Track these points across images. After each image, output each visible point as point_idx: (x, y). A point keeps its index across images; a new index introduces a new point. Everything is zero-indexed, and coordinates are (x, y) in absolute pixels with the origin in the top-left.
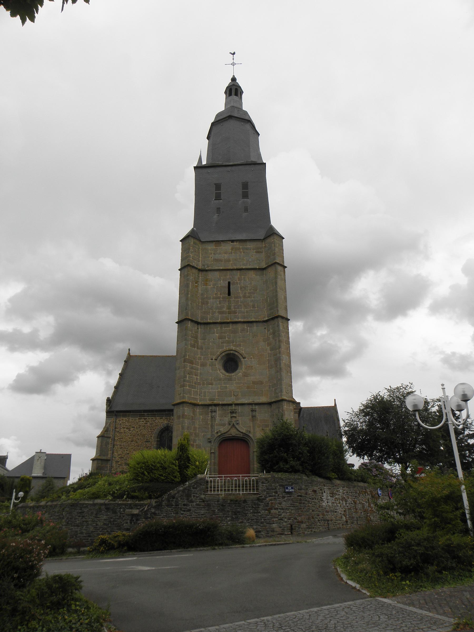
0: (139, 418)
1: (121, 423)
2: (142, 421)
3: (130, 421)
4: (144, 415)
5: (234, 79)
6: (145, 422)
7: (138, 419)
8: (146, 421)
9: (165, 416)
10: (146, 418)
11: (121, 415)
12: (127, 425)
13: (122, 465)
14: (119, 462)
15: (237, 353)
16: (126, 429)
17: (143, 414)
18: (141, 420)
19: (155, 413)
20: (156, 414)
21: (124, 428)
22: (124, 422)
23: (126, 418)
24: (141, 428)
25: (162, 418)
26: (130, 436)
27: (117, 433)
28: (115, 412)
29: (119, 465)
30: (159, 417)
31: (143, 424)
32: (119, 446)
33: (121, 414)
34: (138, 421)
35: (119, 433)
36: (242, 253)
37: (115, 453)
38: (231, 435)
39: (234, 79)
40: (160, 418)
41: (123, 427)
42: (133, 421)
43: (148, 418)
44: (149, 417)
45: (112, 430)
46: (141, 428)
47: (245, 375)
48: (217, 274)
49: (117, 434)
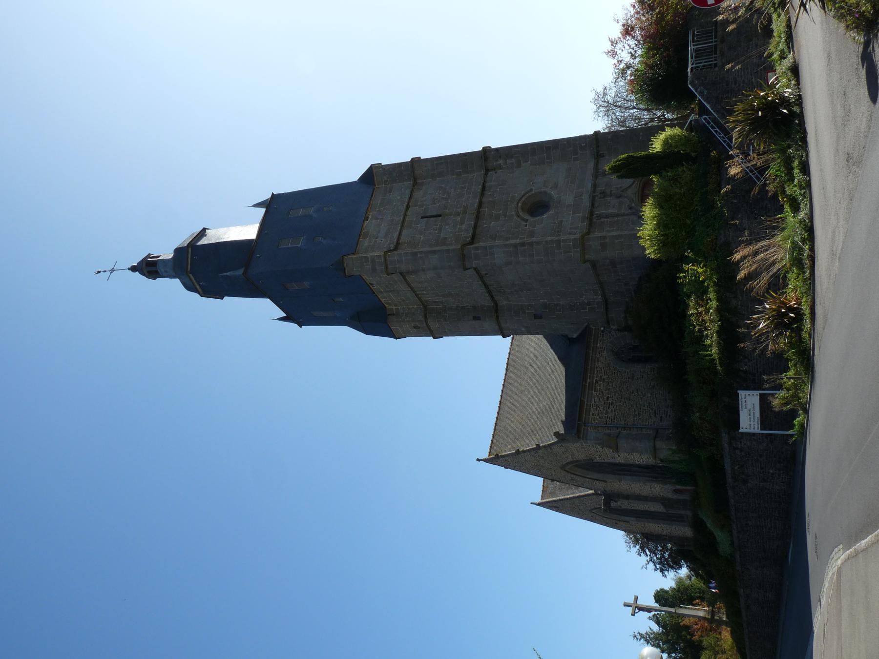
4: (589, 383)
5: (133, 269)
7: (595, 391)
8: (600, 381)
9: (596, 354)
10: (594, 381)
12: (602, 407)
13: (667, 412)
14: (662, 417)
15: (523, 199)
16: (609, 409)
17: (588, 385)
18: (597, 389)
19: (589, 367)
20: (591, 367)
22: (597, 412)
23: (592, 409)
24: (611, 388)
25: (598, 359)
29: (666, 417)
30: (597, 363)
31: (604, 385)
32: (636, 418)
34: (598, 393)
35: (614, 419)
36: (387, 207)
37: (647, 423)
38: (636, 193)
39: (133, 269)
40: (598, 361)
42: (598, 400)
44: (593, 377)
46: (611, 388)
47: (556, 186)
48: (404, 232)
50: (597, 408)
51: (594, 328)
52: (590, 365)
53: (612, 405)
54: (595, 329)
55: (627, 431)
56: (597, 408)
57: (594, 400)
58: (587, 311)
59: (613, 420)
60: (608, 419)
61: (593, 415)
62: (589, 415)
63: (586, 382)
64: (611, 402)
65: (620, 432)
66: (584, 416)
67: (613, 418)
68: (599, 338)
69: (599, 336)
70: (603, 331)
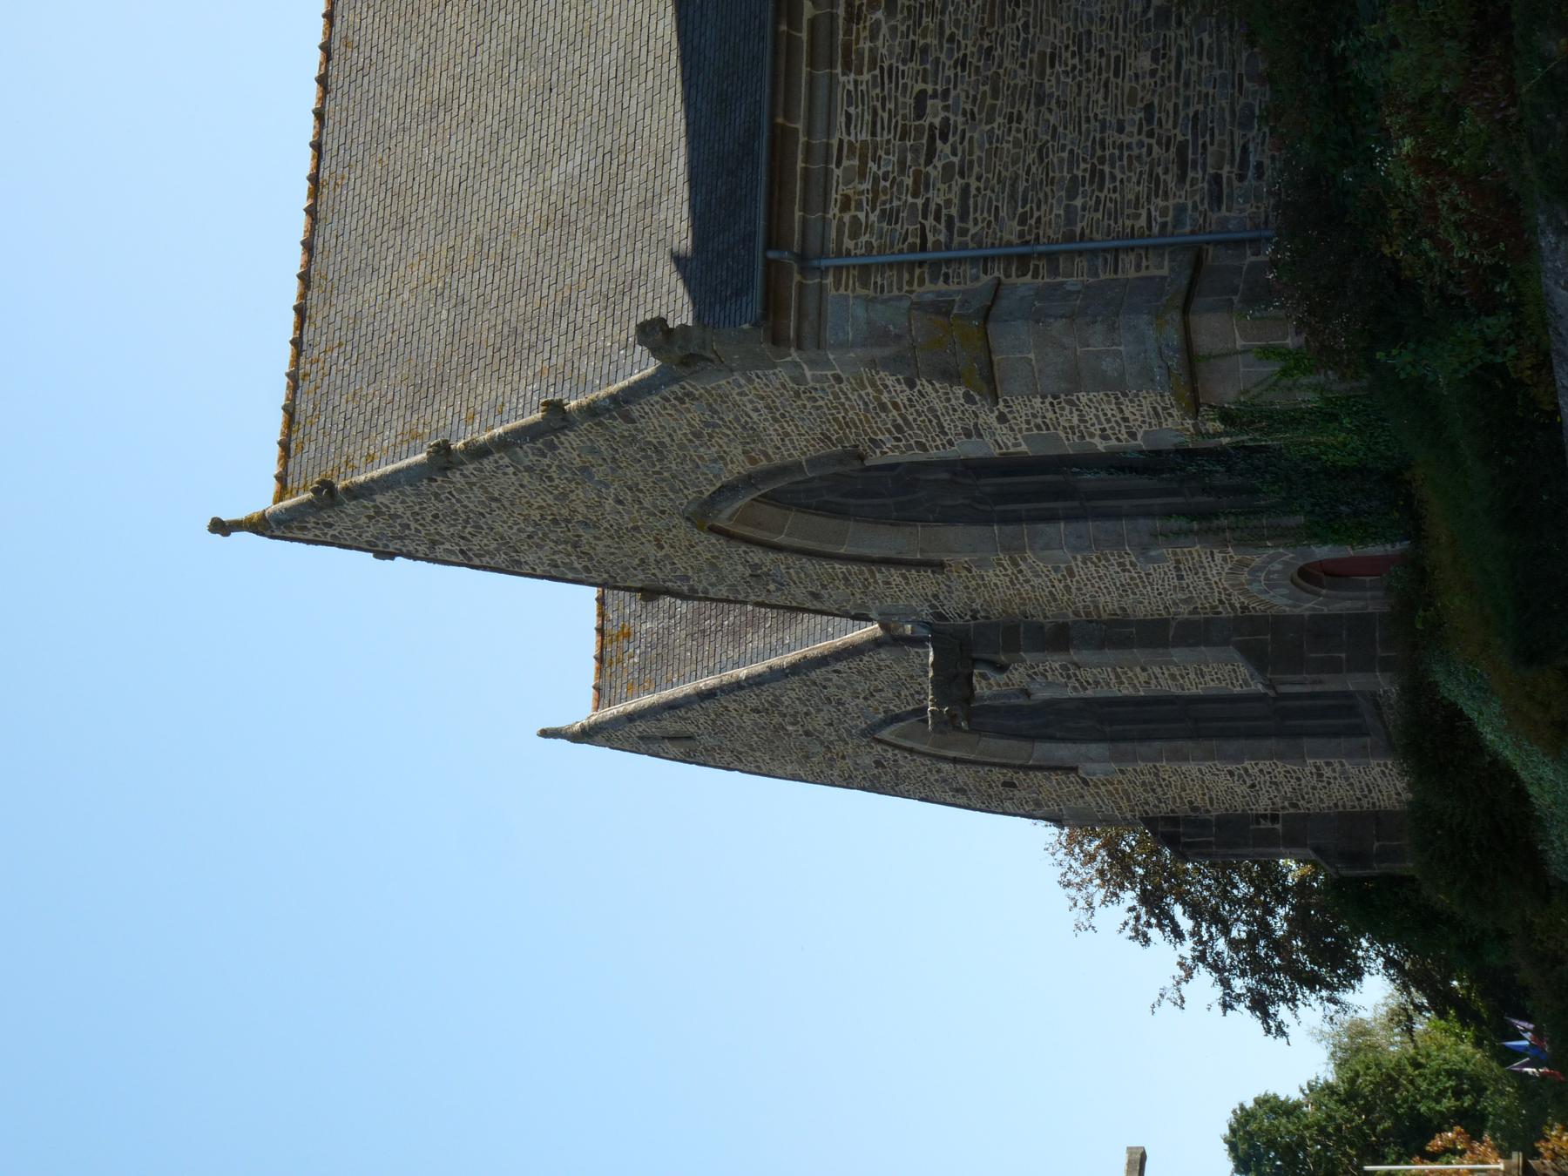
0: (839, 70)
1: (873, 217)
2: (873, 37)
3: (865, 136)
6: (879, 15)
11: (804, 221)
16: (929, 162)
17: (804, 35)
18: (860, 54)
21: (921, 184)
22: (867, 186)
23: (838, 172)
24: (932, 41)
26: (1000, 120)
27: (963, 232)
28: (771, 255)
31: (893, 29)
32: (1078, 202)
33: (798, 214)
34: (866, 76)
35: (964, 216)
41: (915, 195)
45: (934, 280)
46: (932, 41)
49: (972, 231)
50: (863, 163)
53: (944, 139)
55: (1035, 276)
56: (863, 163)
57: (848, 116)
59: (957, 224)
60: (931, 219)
61: (845, 207)
62: (825, 210)
63: (794, 23)
64: (937, 122)
65: (999, 283)
66: (805, 70)
67: (954, 211)
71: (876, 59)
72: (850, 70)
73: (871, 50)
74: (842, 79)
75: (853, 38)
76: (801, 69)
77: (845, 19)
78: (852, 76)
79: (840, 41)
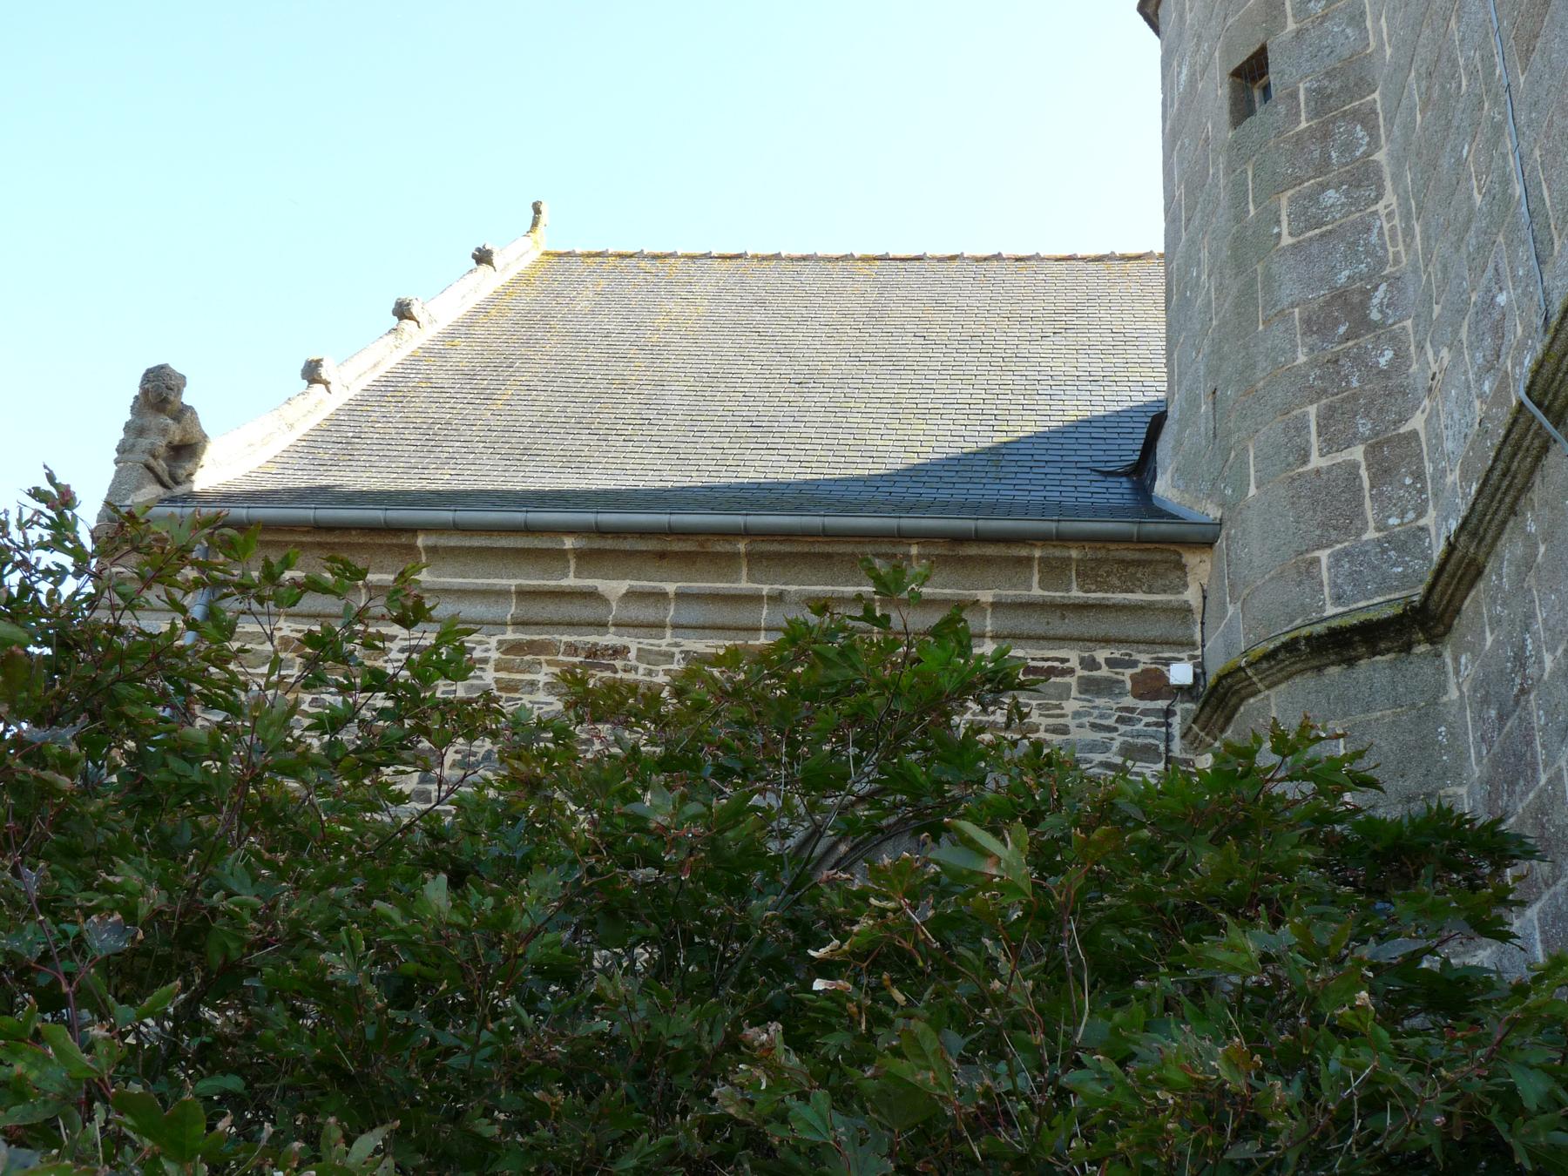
0: (510, 635)
4: (591, 595)
10: (610, 639)
17: (571, 581)
18: (530, 667)
19: (744, 585)
20: (755, 599)
43: (633, 644)
51: (1192, 596)
52: (766, 589)
54: (1186, 610)
58: (1316, 461)
68: (1073, 656)
69: (1101, 655)
70: (1153, 685)
71: (516, 690)
72: (503, 653)
73: (533, 684)
74: (493, 641)
75: (561, 657)
76: (515, 577)
77: (595, 644)
78: (495, 655)
79: (557, 637)
